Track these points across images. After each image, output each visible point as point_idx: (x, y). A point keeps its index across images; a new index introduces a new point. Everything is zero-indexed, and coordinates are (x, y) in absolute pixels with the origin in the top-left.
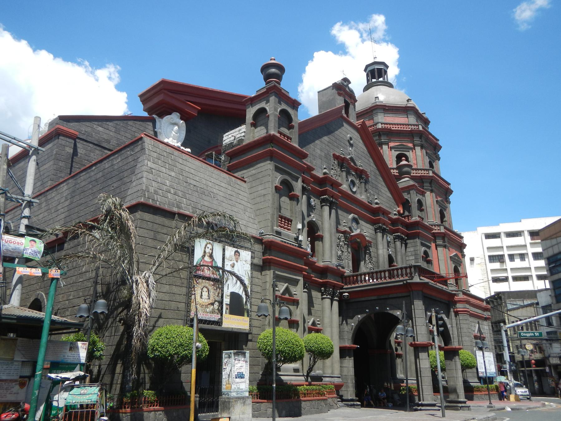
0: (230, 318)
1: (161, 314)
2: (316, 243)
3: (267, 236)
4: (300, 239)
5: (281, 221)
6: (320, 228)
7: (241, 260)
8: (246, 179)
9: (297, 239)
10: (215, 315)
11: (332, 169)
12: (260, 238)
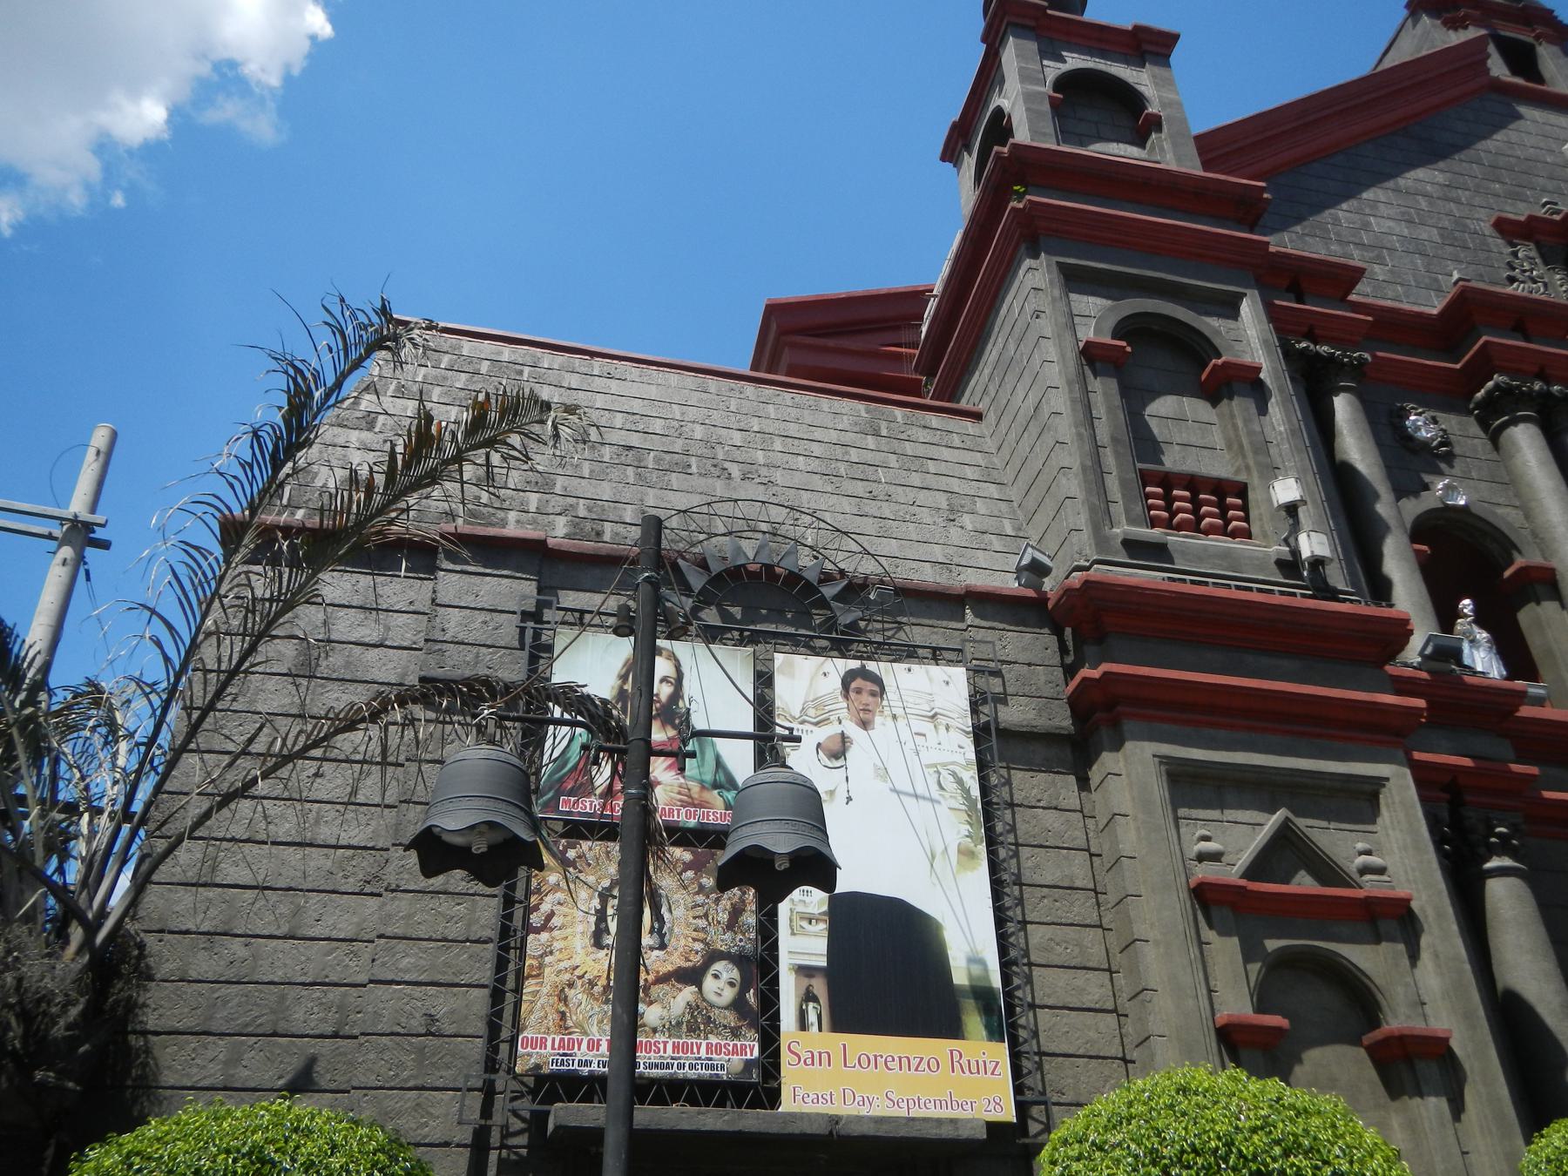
0: (837, 1058)
1: (312, 1061)
2: (1526, 616)
3: (1074, 574)
4: (1306, 553)
5: (1169, 500)
6: (1520, 537)
7: (899, 712)
8: (981, 407)
9: (1290, 566)
10: (713, 1040)
11: (1512, 280)
12: (1031, 593)
